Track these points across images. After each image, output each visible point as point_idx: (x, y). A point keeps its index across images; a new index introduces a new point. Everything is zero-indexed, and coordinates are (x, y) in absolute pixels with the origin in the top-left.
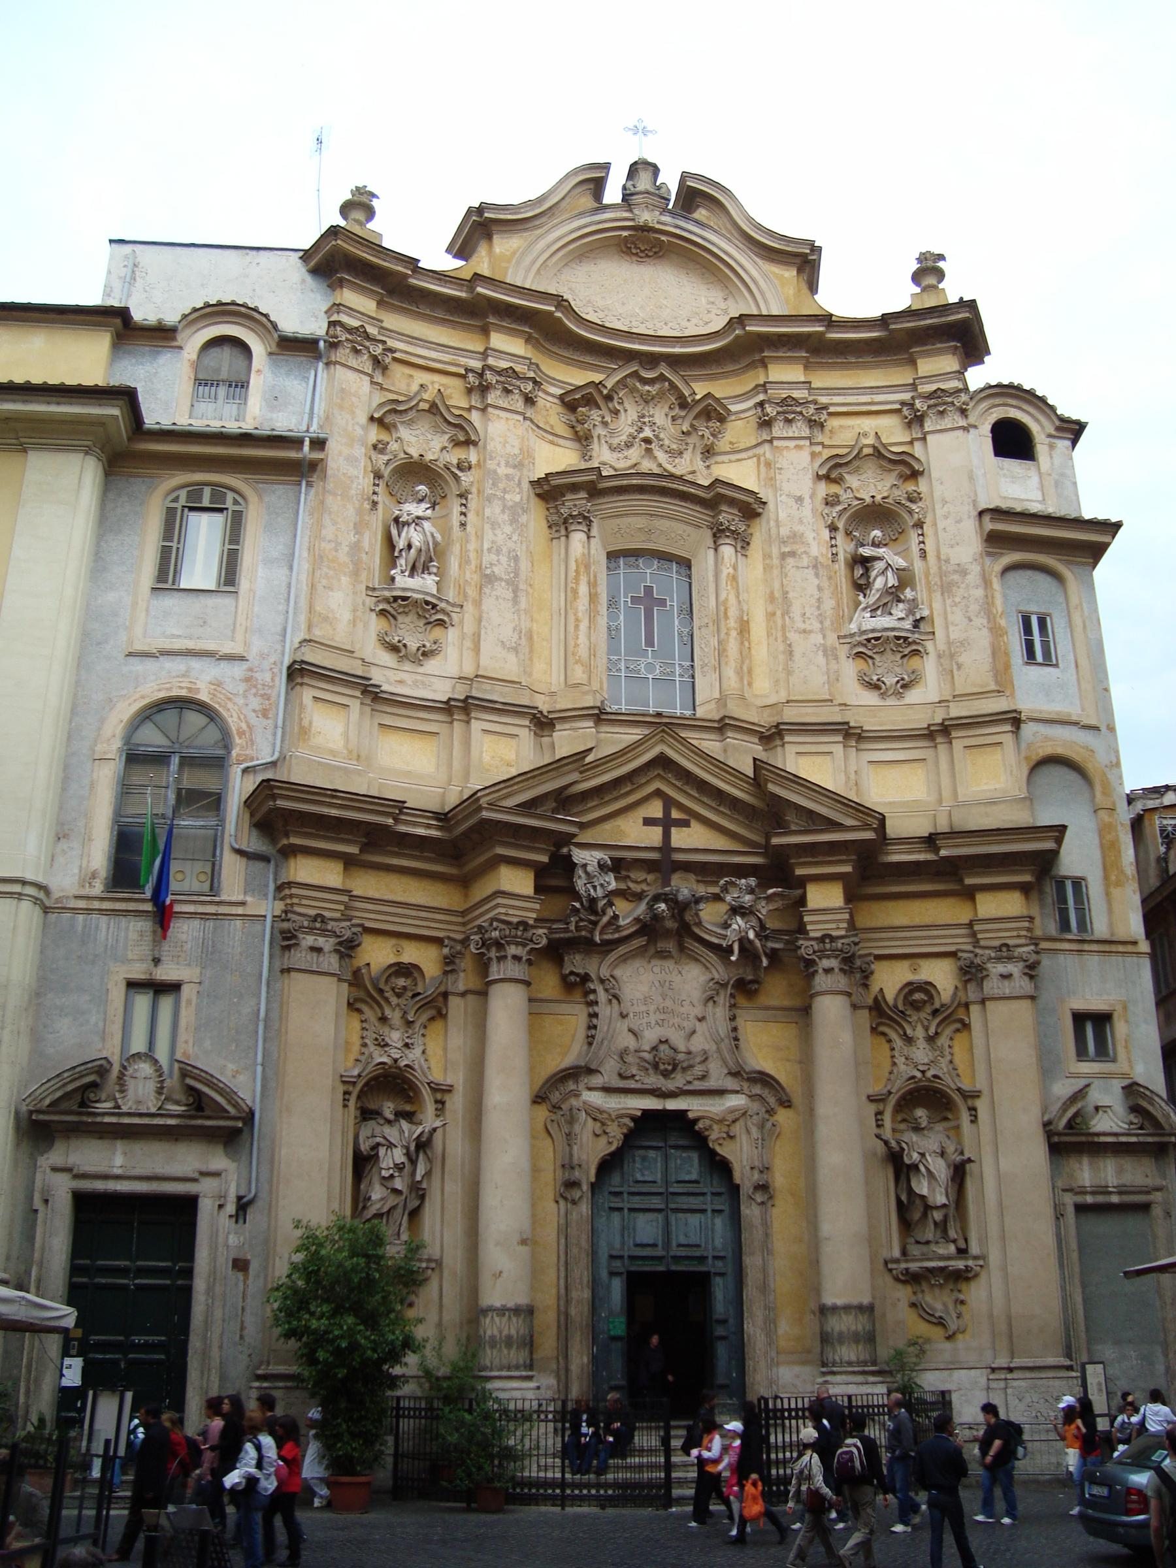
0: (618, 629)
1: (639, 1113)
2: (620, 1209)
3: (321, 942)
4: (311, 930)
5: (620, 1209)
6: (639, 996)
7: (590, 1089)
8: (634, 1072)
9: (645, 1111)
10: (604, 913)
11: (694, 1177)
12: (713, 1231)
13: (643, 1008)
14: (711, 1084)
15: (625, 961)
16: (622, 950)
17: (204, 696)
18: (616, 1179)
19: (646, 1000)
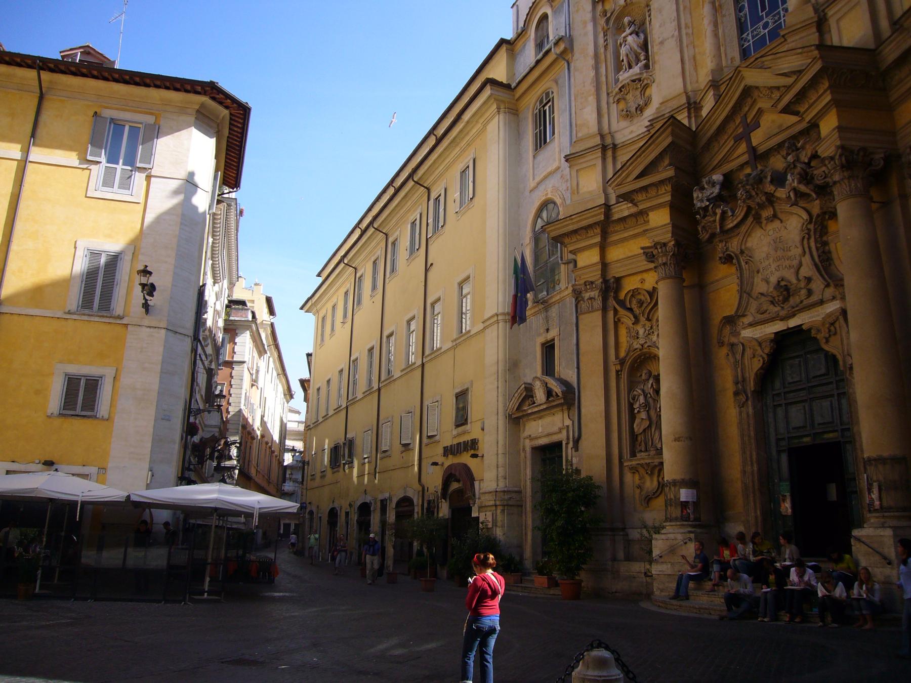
0: (746, 15)
1: (773, 336)
2: (780, 405)
3: (592, 294)
4: (586, 290)
5: (780, 405)
6: (764, 255)
7: (744, 328)
8: (765, 308)
9: (776, 334)
10: (715, 214)
11: (823, 371)
12: (840, 409)
13: (767, 263)
14: (815, 298)
15: (749, 235)
16: (743, 229)
17: (549, 196)
18: (778, 384)
19: (767, 257)
